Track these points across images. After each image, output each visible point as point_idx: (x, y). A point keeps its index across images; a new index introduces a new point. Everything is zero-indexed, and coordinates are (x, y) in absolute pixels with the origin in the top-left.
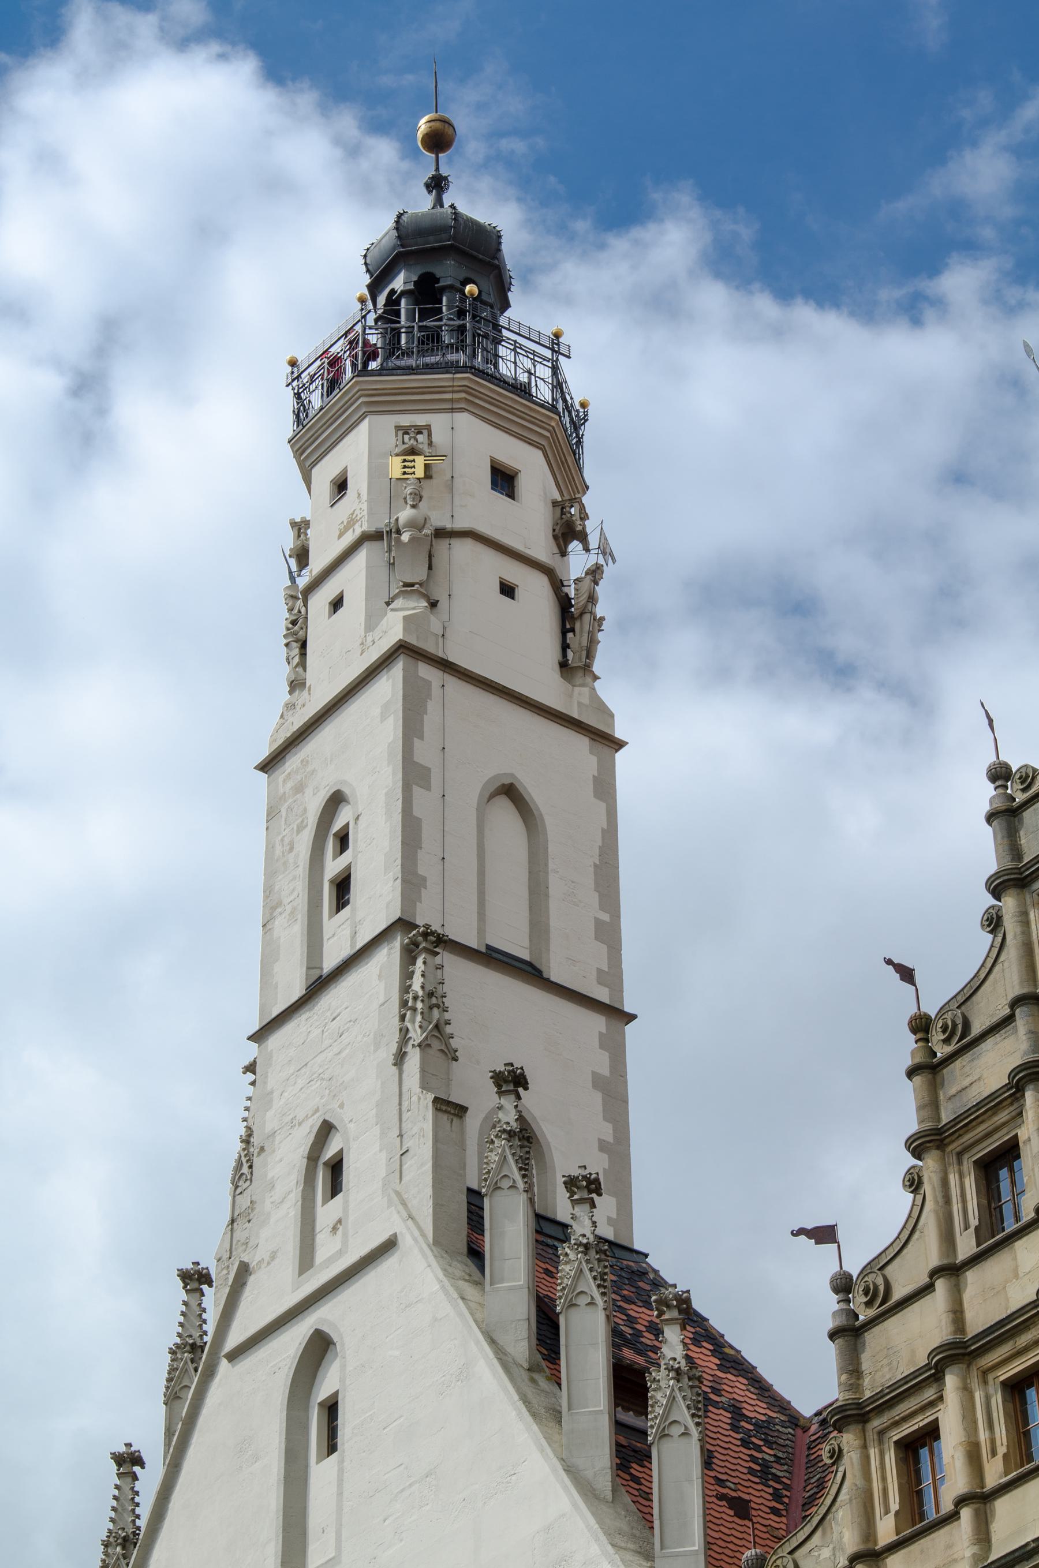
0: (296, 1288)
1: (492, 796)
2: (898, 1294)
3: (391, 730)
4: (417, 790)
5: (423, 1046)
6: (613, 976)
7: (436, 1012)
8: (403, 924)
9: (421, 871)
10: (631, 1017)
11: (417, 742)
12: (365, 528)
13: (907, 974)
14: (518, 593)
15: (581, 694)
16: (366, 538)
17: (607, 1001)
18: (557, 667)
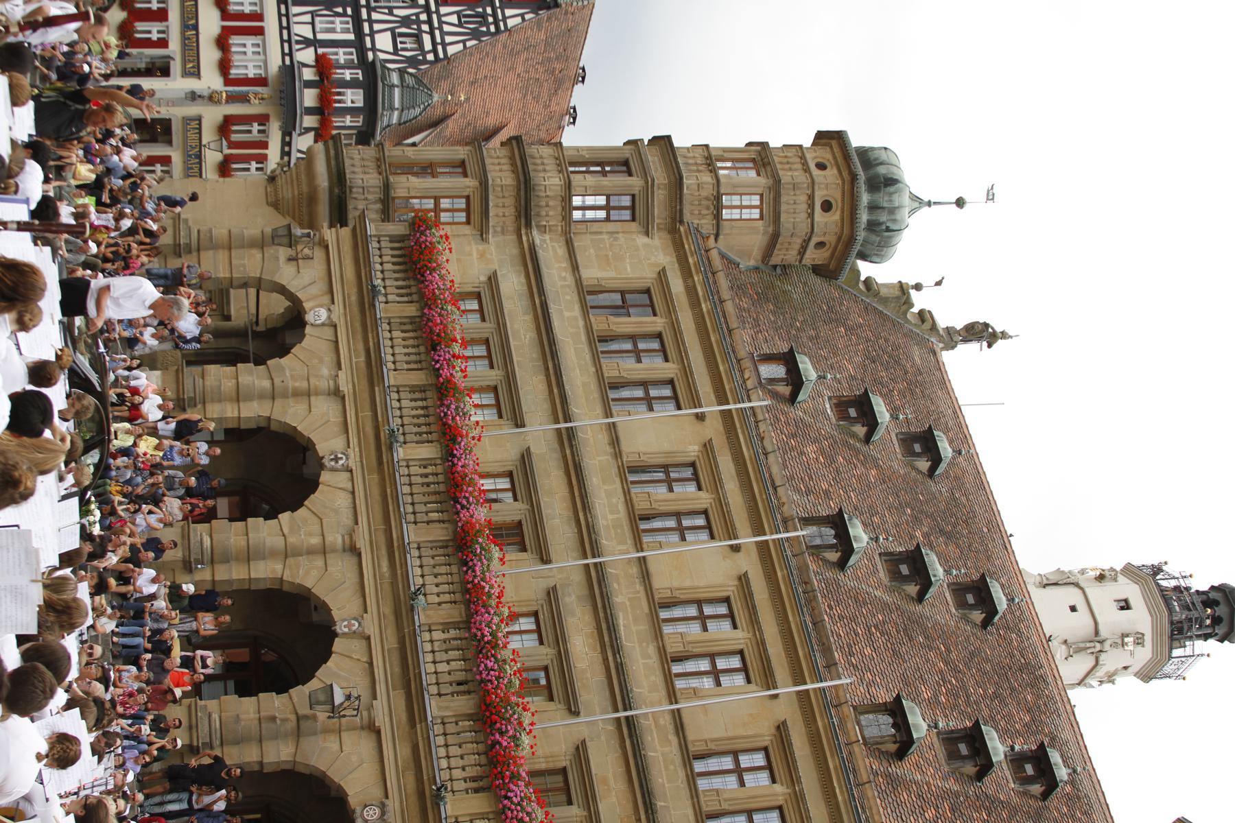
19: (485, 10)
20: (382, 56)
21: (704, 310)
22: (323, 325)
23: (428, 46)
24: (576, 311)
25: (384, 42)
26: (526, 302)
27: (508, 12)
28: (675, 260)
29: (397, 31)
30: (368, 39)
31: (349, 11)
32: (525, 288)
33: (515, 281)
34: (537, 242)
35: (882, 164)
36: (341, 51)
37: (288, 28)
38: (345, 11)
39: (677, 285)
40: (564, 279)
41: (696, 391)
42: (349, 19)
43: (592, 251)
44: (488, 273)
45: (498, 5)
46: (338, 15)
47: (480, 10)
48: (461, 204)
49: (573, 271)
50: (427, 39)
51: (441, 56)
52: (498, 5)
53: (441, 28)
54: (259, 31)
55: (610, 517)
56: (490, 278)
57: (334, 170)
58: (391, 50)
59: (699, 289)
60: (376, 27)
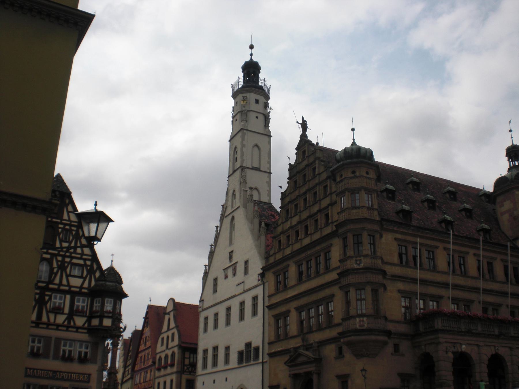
0: (231, 210)
1: (254, 147)
3: (240, 140)
4: (244, 148)
5: (243, 182)
6: (270, 168)
7: (245, 178)
8: (241, 166)
9: (244, 159)
10: (272, 173)
11: (244, 141)
12: (239, 111)
13: (281, 187)
14: (259, 118)
15: (267, 130)
16: (239, 112)
17: (269, 171)
18: (264, 127)
19: (60, 228)
20: (86, 285)
22: (466, 346)
23: (81, 262)
25: (76, 282)
27: (65, 217)
29: (68, 273)
30: (73, 289)
31: (49, 293)
35: (366, 154)
36: (95, 304)
37: (58, 326)
38: (48, 295)
39: (399, 236)
42: (53, 295)
45: (59, 221)
46: (50, 299)
47: (60, 230)
48: (359, 292)
50: (74, 261)
51: (90, 258)
52: (59, 221)
53: (71, 253)
54: (58, 340)
58: (81, 280)
59: (405, 231)
60: (65, 282)
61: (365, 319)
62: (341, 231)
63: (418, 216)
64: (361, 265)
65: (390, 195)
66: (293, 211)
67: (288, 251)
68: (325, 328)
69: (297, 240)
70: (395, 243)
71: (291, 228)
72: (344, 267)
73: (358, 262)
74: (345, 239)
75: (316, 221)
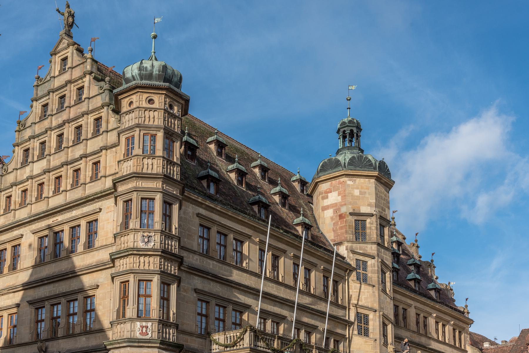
2: (9, 171)
21: (219, 209)
24: (211, 262)
26: (206, 281)
28: (191, 205)
32: (200, 278)
33: (197, 281)
34: (187, 264)
40: (197, 259)
41: (238, 231)
43: (186, 240)
44: (193, 292)
49: (194, 253)
55: (275, 289)
56: (196, 292)
57: (174, 349)
59: (211, 205)
61: (149, 324)
62: (121, 188)
63: (224, 190)
64: (150, 245)
65: (189, 153)
66: (37, 153)
67: (22, 214)
68: (80, 335)
69: (40, 197)
70: (197, 221)
71: (32, 178)
72: (123, 245)
73: (146, 240)
74: (128, 202)
75: (77, 171)
